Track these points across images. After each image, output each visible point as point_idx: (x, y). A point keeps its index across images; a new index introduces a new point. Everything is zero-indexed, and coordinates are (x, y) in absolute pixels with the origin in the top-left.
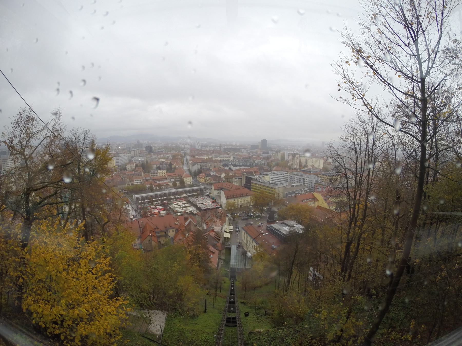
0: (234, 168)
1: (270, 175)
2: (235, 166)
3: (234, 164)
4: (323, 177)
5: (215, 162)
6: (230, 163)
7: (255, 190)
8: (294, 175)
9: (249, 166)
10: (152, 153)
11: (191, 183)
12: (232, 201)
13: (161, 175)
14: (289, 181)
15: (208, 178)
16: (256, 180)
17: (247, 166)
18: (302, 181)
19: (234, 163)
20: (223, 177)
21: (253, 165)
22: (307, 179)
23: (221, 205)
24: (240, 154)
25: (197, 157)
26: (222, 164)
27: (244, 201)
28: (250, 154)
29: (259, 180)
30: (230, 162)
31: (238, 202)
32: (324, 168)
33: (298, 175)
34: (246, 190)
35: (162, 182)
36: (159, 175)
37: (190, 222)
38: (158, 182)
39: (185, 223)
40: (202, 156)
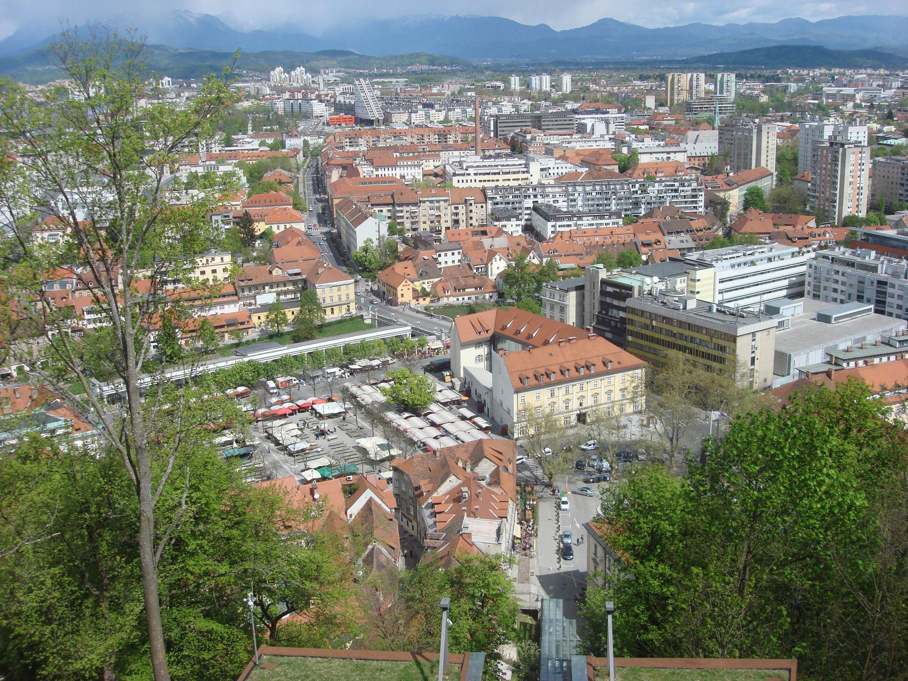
6: (529, 203)
9: (618, 214)
11: (353, 311)
14: (807, 288)
15: (427, 285)
24: (578, 144)
25: (365, 170)
27: (596, 395)
31: (567, 401)
34: (602, 347)
37: (371, 500)
39: (349, 512)
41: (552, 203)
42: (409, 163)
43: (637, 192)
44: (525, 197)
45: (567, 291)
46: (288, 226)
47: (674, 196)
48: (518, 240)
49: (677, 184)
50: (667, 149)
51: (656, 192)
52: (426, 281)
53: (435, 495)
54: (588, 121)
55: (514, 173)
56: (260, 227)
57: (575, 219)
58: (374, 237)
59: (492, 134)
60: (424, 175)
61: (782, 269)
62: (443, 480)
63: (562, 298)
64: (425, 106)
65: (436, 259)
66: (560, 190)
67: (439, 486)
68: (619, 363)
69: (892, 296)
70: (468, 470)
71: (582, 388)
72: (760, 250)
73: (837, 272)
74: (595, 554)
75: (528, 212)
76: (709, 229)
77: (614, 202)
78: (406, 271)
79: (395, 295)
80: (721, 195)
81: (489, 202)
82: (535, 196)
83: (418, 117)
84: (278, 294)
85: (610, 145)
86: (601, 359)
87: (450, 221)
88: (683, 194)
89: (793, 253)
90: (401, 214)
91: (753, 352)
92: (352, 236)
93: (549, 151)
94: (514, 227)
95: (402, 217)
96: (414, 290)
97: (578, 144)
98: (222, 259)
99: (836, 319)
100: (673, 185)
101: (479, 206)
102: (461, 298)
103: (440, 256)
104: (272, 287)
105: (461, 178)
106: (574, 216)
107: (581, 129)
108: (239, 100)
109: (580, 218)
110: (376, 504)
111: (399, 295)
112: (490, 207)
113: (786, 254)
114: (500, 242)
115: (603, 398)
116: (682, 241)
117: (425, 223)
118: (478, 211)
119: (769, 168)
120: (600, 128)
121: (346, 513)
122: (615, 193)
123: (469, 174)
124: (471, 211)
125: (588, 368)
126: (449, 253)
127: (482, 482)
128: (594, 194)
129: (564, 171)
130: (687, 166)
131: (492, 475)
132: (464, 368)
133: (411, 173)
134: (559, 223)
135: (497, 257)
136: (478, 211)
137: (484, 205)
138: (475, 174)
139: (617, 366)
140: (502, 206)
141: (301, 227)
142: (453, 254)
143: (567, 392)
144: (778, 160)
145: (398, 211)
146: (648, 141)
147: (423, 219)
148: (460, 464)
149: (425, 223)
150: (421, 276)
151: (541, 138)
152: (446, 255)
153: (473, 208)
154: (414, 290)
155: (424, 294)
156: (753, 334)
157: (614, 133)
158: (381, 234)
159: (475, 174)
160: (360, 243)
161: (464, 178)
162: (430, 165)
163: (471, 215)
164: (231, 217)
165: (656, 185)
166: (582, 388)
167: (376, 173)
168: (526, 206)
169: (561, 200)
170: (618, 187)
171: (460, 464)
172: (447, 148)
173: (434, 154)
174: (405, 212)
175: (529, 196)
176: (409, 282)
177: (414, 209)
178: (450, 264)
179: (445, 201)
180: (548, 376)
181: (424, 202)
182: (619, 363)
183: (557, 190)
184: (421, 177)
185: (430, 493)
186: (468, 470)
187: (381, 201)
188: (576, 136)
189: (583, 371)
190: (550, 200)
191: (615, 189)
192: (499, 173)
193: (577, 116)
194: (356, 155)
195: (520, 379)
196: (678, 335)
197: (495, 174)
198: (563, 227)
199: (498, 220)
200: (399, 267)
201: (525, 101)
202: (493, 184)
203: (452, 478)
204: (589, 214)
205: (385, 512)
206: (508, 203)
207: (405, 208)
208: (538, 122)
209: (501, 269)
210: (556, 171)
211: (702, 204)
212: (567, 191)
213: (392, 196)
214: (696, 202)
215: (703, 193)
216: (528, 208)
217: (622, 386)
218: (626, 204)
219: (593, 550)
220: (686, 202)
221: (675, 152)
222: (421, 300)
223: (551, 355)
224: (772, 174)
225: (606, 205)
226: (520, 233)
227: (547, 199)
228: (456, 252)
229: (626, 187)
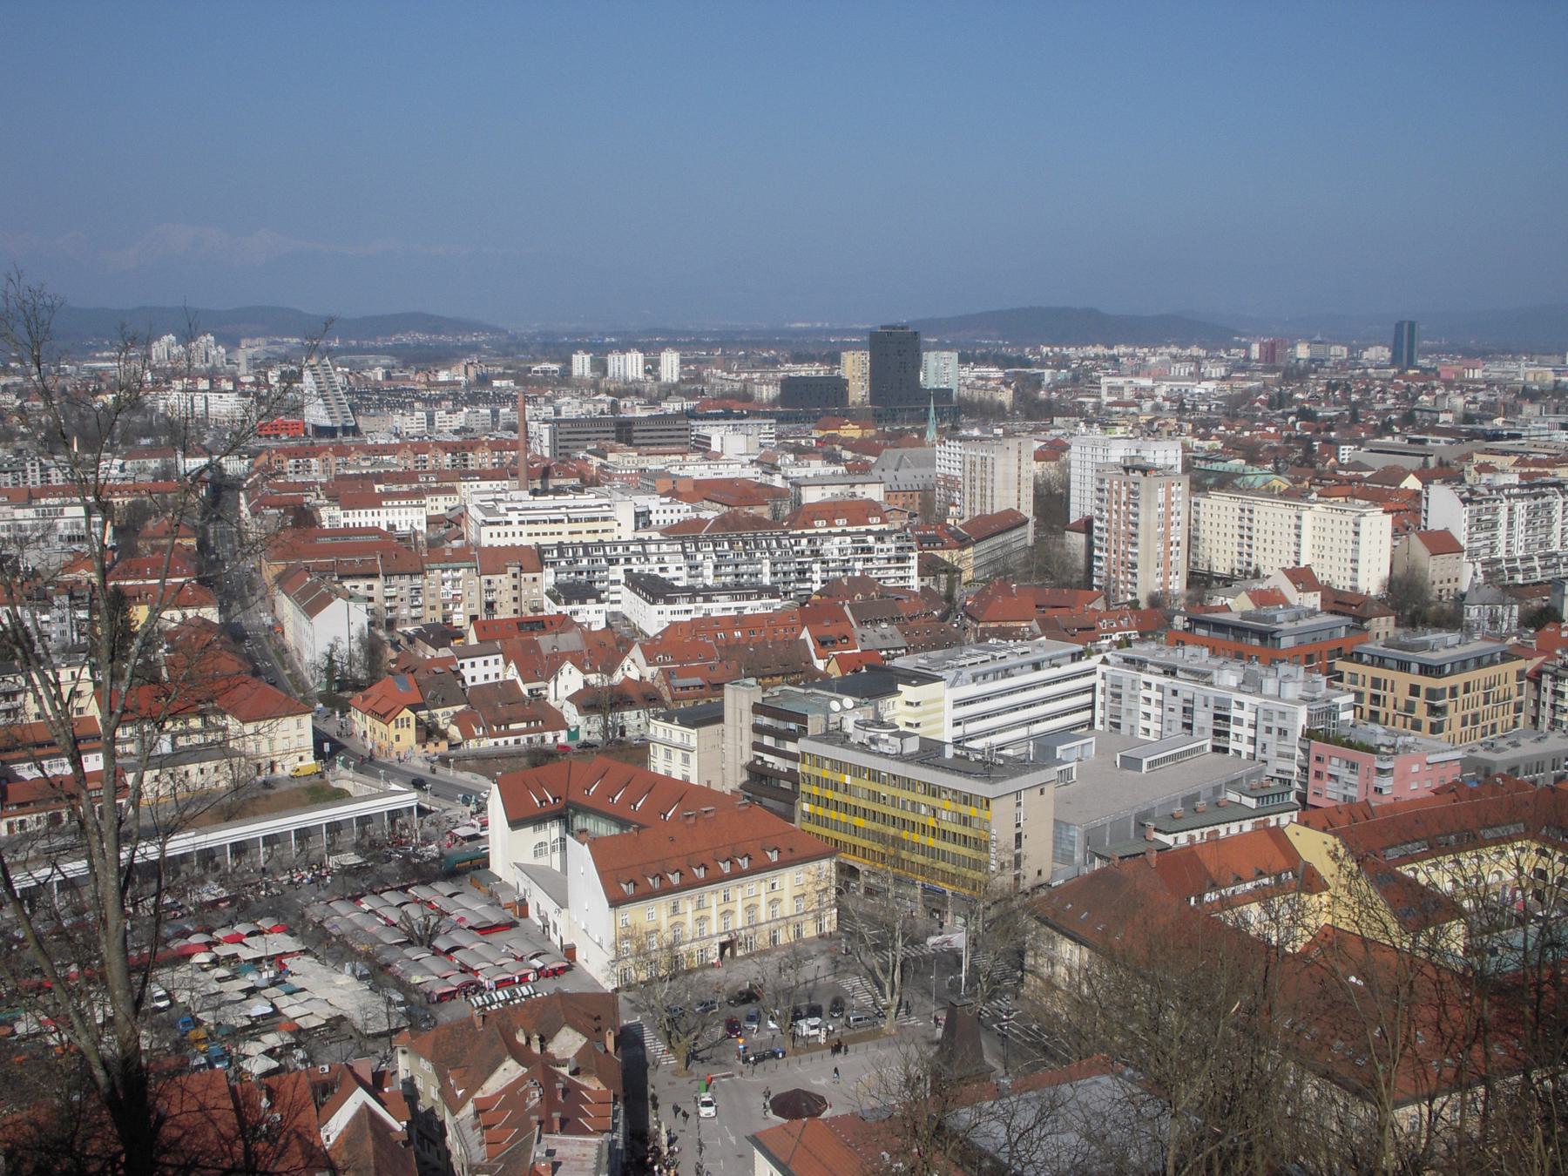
0: (653, 618)
1: (949, 675)
2: (655, 589)
3: (652, 579)
4: (1376, 683)
5: (493, 561)
7: (833, 815)
8: (1138, 664)
9: (772, 592)
12: (654, 916)
16: (835, 736)
17: (762, 591)
18: (1203, 718)
19: (651, 568)
20: (563, 693)
22: (1246, 699)
23: (570, 952)
24: (697, 469)
25: (331, 516)
26: (548, 578)
27: (751, 908)
28: (774, 468)
29: (859, 736)
30: (612, 562)
32: (1392, 584)
33: (1170, 672)
40: (374, 502)
41: (657, 572)
43: (803, 552)
50: (851, 479)
51: (836, 552)
53: (478, 1095)
57: (700, 599)
61: (1057, 681)
64: (428, 401)
67: (486, 1079)
69: (1239, 722)
71: (726, 898)
72: (1020, 650)
73: (1148, 685)
82: (628, 561)
87: (477, 603)
89: (1073, 655)
91: (1018, 825)
94: (592, 615)
99: (1150, 764)
101: (529, 576)
102: (501, 741)
103: (462, 666)
105: (495, 529)
107: (702, 446)
108: (97, 392)
109: (707, 599)
113: (1064, 655)
115: (763, 914)
117: (433, 608)
119: (1022, 511)
126: (479, 661)
129: (676, 517)
133: (407, 518)
135: (568, 666)
138: (521, 523)
139: (788, 856)
144: (1037, 497)
147: (431, 601)
149: (433, 608)
156: (1018, 793)
159: (521, 523)
161: (502, 529)
162: (440, 505)
166: (726, 898)
167: (343, 520)
168: (612, 577)
171: (521, 1039)
172: (466, 475)
173: (446, 482)
175: (618, 561)
178: (480, 681)
184: (423, 528)
186: (536, 1049)
192: (561, 521)
194: (305, 487)
196: (889, 800)
197: (555, 521)
201: (602, 396)
202: (555, 540)
204: (724, 589)
210: (661, 517)
211: (914, 572)
215: (915, 555)
217: (799, 891)
221: (864, 484)
224: (1025, 522)
228: (491, 659)
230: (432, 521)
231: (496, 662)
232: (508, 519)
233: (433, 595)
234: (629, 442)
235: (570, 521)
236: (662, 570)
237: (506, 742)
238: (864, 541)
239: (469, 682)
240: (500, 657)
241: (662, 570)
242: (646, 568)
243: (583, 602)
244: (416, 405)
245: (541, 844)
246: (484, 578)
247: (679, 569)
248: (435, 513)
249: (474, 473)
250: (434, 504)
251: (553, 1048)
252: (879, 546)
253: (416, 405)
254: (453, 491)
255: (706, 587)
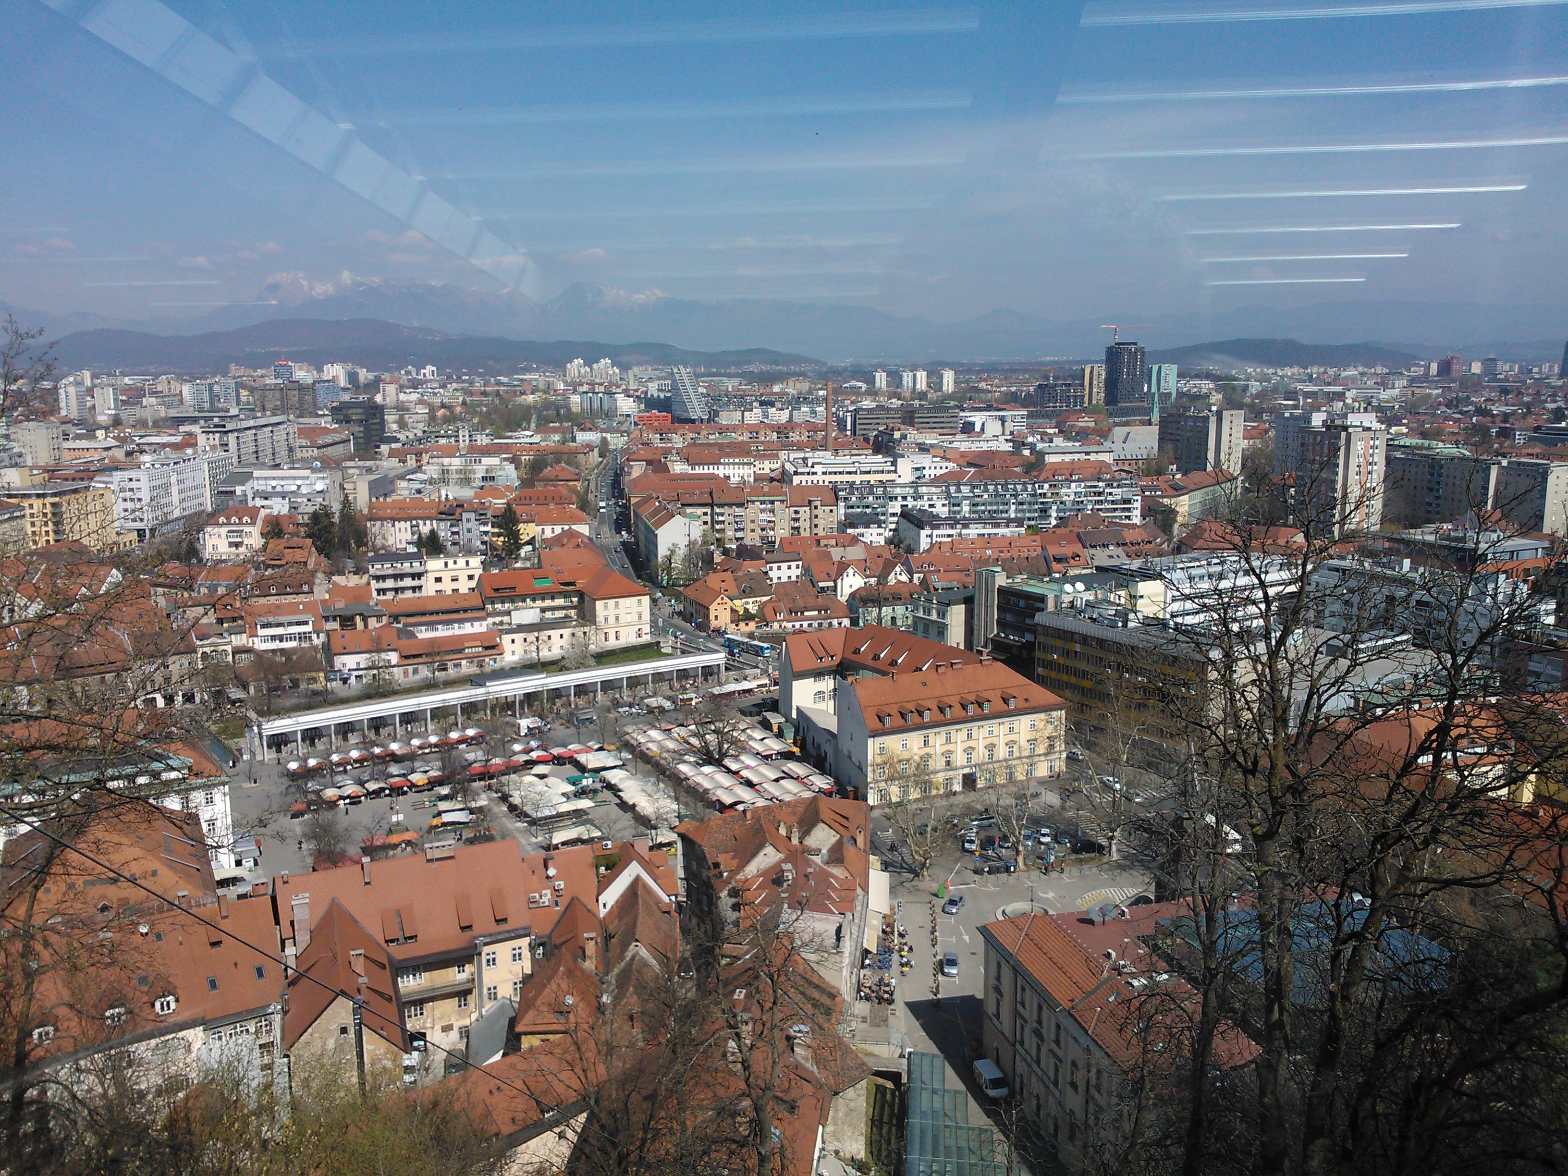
6: (895, 507)
9: (1019, 522)
10: (384, 448)
13: (447, 587)
17: (1009, 522)
21: (1044, 512)
24: (963, 444)
25: (679, 468)
27: (991, 747)
35: (456, 630)
36: (430, 588)
37: (637, 879)
38: (424, 634)
39: (602, 899)
41: (926, 507)
42: (737, 460)
44: (891, 499)
45: (948, 605)
46: (566, 527)
47: (1097, 502)
48: (880, 551)
49: (1101, 484)
52: (751, 600)
54: (977, 419)
55: (876, 472)
56: (528, 530)
57: (959, 526)
58: (683, 542)
59: (849, 433)
60: (755, 480)
62: (754, 855)
63: (942, 614)
64: (762, 404)
65: (766, 573)
66: (939, 490)
67: (748, 862)
68: (1026, 700)
70: (795, 841)
71: (969, 736)
74: (998, 978)
75: (895, 519)
76: (1150, 542)
77: (1013, 507)
78: (722, 585)
79: (707, 617)
80: (1166, 501)
81: (842, 504)
82: (904, 498)
83: (754, 416)
84: (543, 610)
85: (1008, 447)
86: (999, 693)
88: (1110, 498)
90: (721, 518)
92: (652, 540)
93: (923, 449)
94: (876, 536)
95: (723, 522)
96: (733, 611)
97: (963, 444)
98: (467, 563)
100: (1095, 487)
101: (828, 509)
102: (797, 625)
104: (534, 600)
106: (957, 522)
107: (968, 428)
108: (523, 393)
109: (965, 526)
110: (646, 886)
111: (712, 617)
112: (842, 511)
114: (855, 553)
115: (1002, 752)
116: (1111, 557)
118: (826, 517)
120: (993, 428)
121: (597, 901)
122: (1015, 496)
123: (815, 473)
124: (816, 517)
125: (980, 705)
126: (784, 566)
127: (814, 858)
128: (986, 496)
129: (944, 471)
130: (1115, 469)
131: (831, 850)
132: (798, 709)
134: (936, 532)
135: (850, 571)
136: (826, 517)
137: (834, 508)
138: (824, 473)
139: (1023, 704)
140: (859, 510)
141: (584, 529)
142: (789, 568)
143: (948, 741)
145: (718, 514)
146: (1059, 441)
147: (752, 526)
148: (783, 831)
149: (753, 531)
150: (744, 593)
151: (914, 435)
152: (779, 568)
153: (819, 512)
154: (733, 611)
155: (748, 617)
157: (1012, 433)
158: (692, 538)
159: (824, 473)
160: (662, 551)
163: (816, 521)
164: (489, 516)
165: (1073, 485)
166: (969, 736)
168: (891, 511)
169: (939, 504)
170: (1019, 487)
171: (783, 831)
172: (789, 446)
173: (770, 453)
174: (726, 515)
175: (896, 498)
176: (726, 599)
177: (738, 511)
178: (784, 579)
179: (782, 501)
180: (920, 714)
181: (753, 502)
182: (1026, 700)
183: (934, 490)
184: (752, 479)
185: (733, 872)
186: (795, 841)
187: (695, 499)
188: (959, 437)
189: (972, 710)
190: (924, 504)
191: (1015, 490)
192: (856, 473)
193: (962, 414)
194: (667, 452)
195: (879, 717)
197: (850, 473)
198: (942, 535)
199: (853, 526)
200: (713, 580)
201: (893, 400)
203: (769, 849)
205: (658, 901)
206: (867, 507)
207: (726, 510)
208: (909, 417)
209: (855, 588)
210: (933, 472)
211: (1137, 513)
212: (948, 492)
213: (711, 494)
214: (1129, 510)
215: (1139, 498)
216: (893, 515)
218: (1030, 511)
219: (993, 972)
220: (1115, 510)
221: (1097, 452)
222: (742, 625)
223: (925, 684)
225: (1002, 512)
226: (883, 543)
227: (919, 503)
228: (793, 564)
229: (1030, 487)
230: (758, 478)
231: (798, 567)
232: (813, 470)
233: (753, 521)
234: (912, 424)
235: (862, 473)
236: (931, 506)
237: (801, 626)
238: (1095, 487)
239: (775, 581)
240: (800, 563)
241: (931, 506)
242: (919, 503)
243: (867, 526)
244: (755, 404)
245: (819, 692)
246: (792, 509)
247: (944, 505)
248: (762, 472)
249: (793, 444)
250: (762, 466)
251: (811, 841)
252: (1108, 490)
253: (755, 404)
254: (777, 457)
255: (964, 518)
